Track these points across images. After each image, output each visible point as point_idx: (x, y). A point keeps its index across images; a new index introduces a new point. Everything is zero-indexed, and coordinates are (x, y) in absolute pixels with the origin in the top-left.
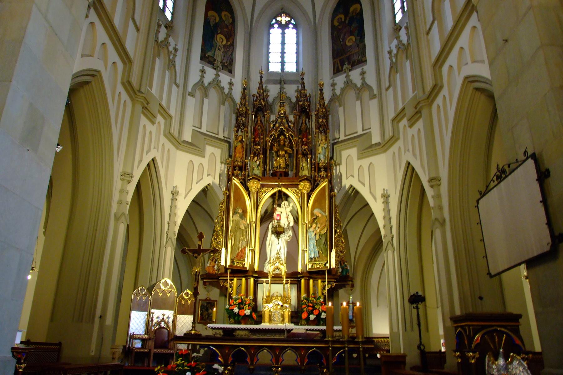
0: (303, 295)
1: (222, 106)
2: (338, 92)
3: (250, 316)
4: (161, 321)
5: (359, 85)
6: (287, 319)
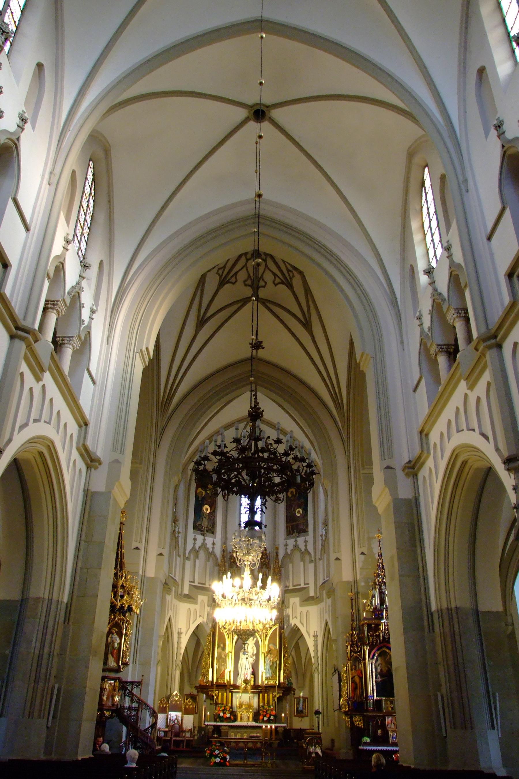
0: (261, 704)
1: (208, 562)
2: (289, 552)
3: (230, 718)
4: (175, 720)
5: (303, 550)
6: (251, 719)
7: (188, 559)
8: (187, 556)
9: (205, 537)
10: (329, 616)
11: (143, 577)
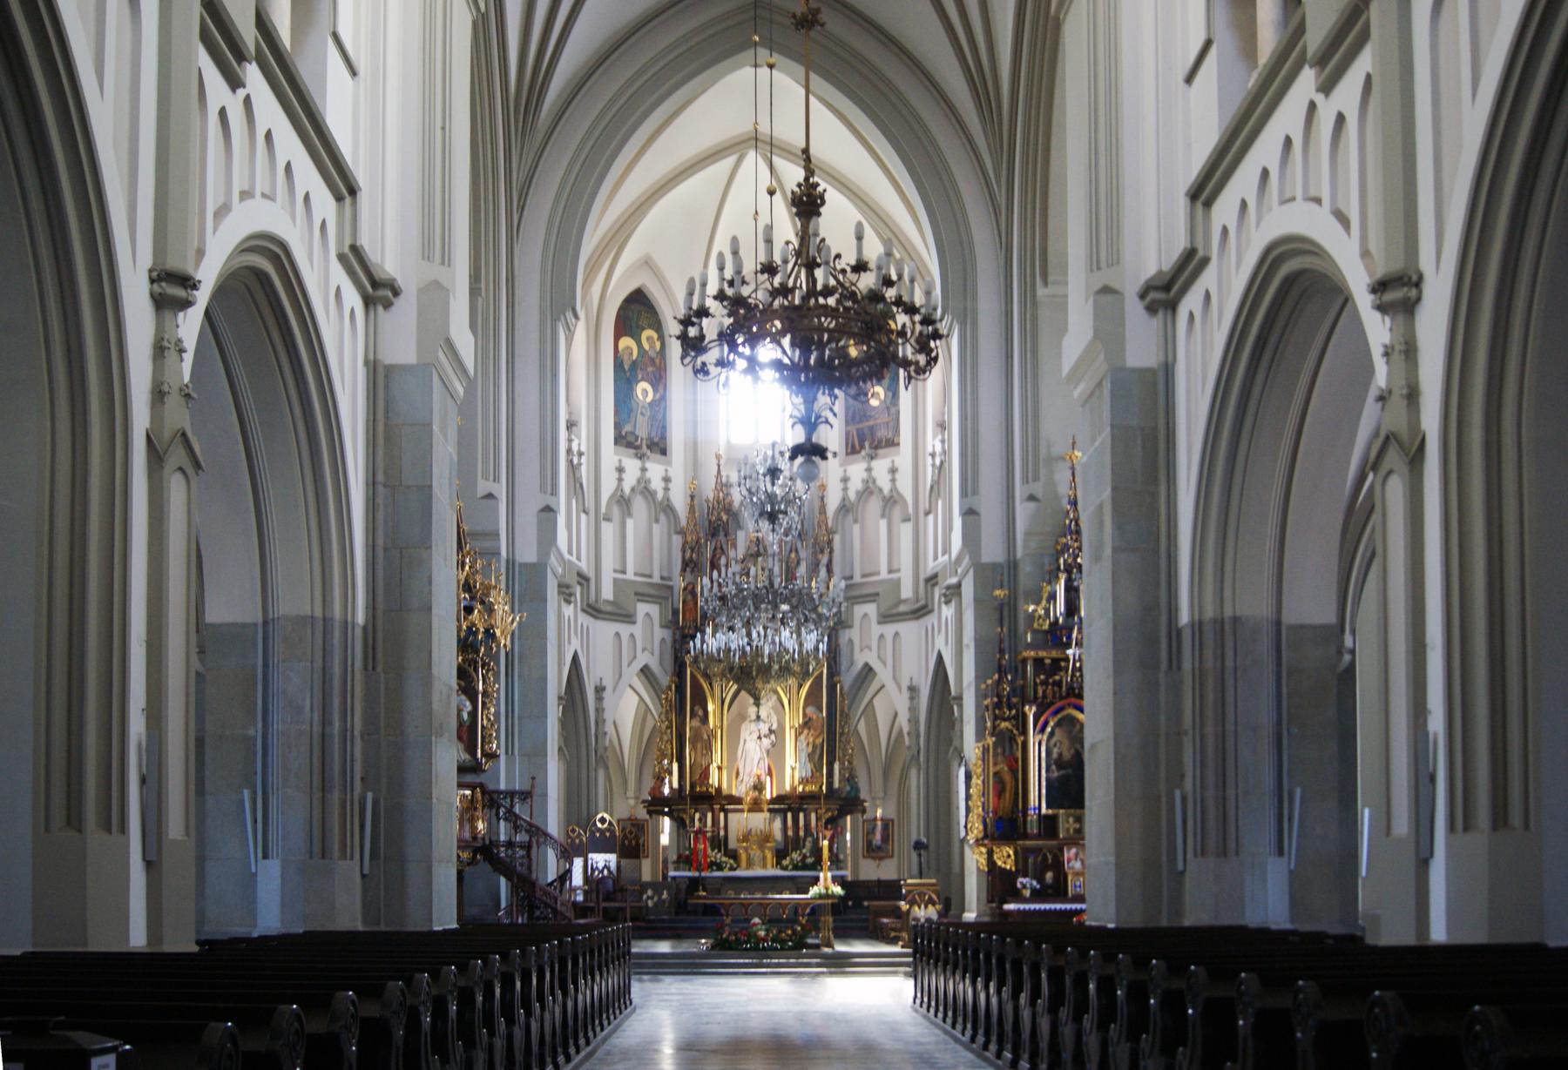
2: (852, 495)
6: (769, 865)
7: (608, 519)
8: (603, 510)
9: (643, 463)
10: (947, 643)
11: (511, 563)
